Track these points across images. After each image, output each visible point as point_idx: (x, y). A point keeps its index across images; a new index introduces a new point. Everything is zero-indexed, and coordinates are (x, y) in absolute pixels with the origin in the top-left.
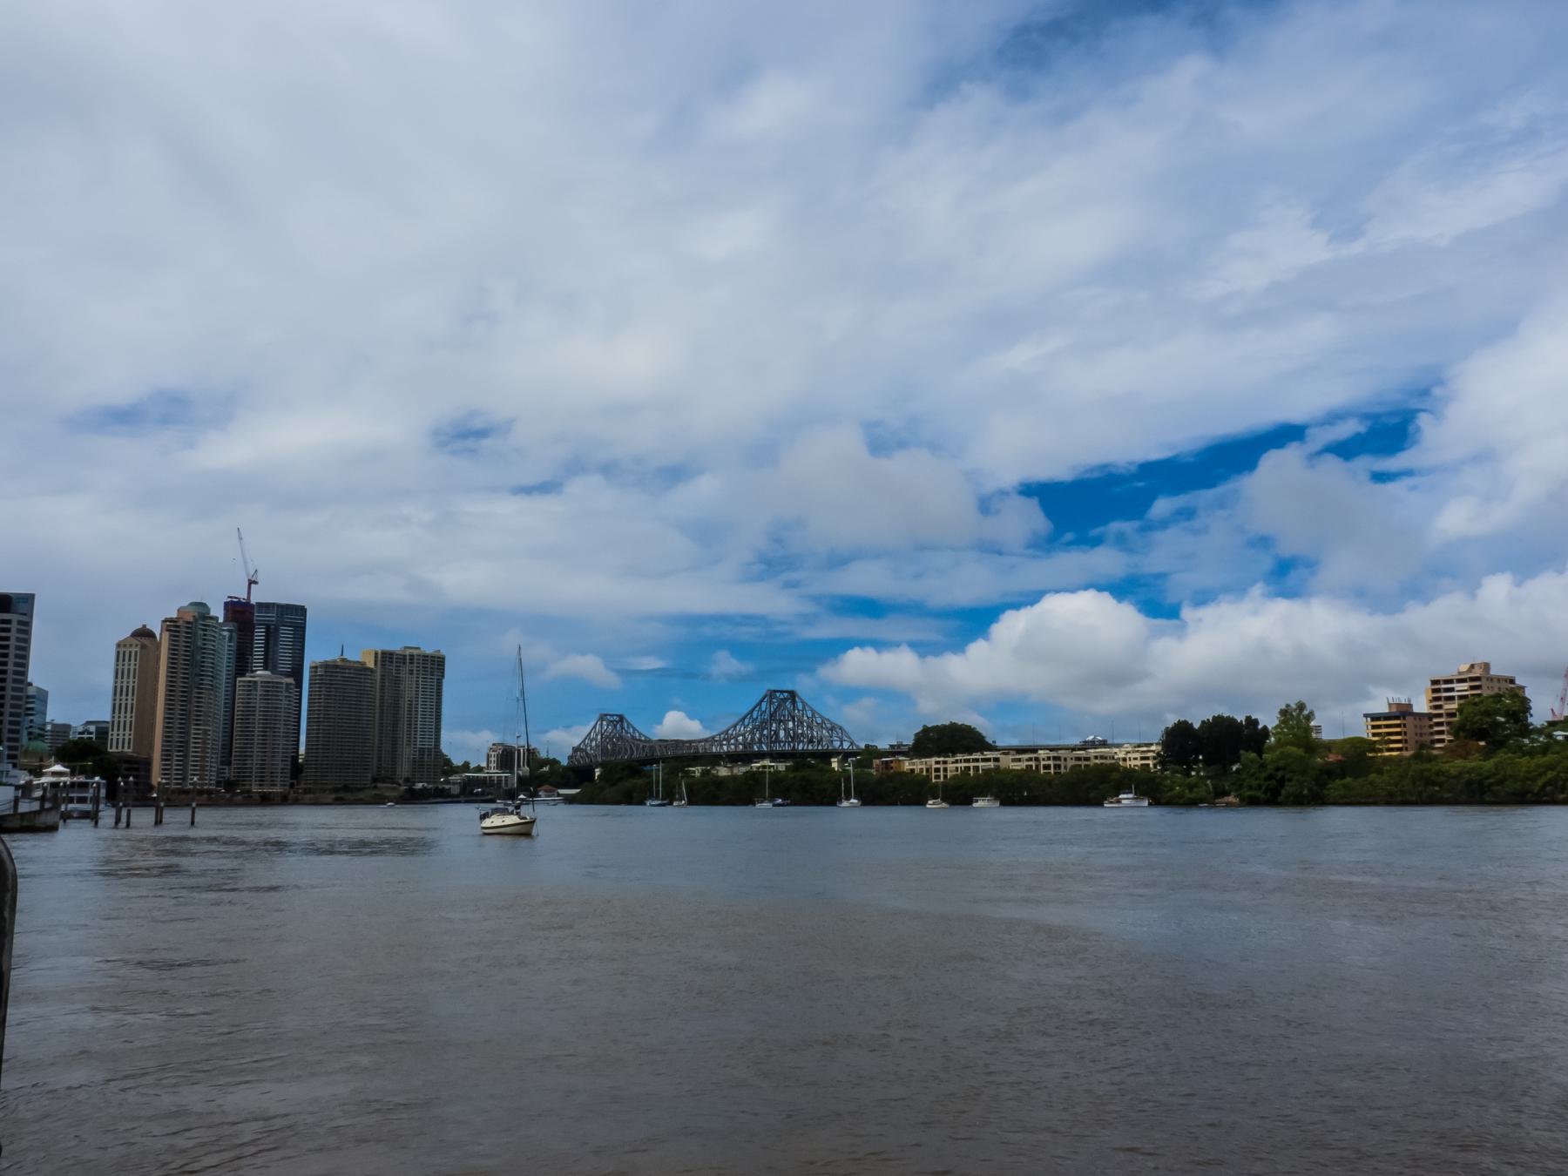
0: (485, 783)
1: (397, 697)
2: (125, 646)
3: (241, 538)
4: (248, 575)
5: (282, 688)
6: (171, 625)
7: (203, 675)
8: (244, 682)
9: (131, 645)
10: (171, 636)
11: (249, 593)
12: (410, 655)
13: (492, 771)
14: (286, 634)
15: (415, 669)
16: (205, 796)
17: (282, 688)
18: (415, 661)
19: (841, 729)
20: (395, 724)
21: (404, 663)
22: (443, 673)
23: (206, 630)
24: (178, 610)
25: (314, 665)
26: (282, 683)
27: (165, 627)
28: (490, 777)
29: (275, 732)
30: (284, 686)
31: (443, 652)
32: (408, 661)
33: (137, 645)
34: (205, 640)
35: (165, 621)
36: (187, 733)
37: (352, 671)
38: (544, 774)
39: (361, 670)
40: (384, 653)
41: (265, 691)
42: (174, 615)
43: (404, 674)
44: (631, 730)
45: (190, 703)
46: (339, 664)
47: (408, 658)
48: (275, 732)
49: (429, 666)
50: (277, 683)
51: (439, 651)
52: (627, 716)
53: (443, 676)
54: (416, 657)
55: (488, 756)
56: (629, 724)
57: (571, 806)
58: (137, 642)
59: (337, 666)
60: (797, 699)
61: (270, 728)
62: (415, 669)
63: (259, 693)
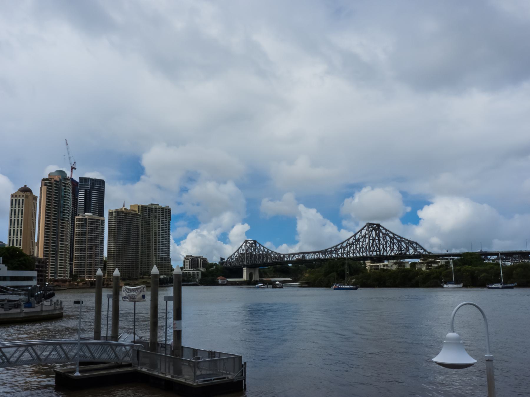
0: (187, 276)
1: (149, 229)
2: (16, 196)
3: (67, 145)
4: (71, 164)
5: (99, 222)
6: (47, 182)
7: (64, 212)
8: (79, 219)
9: (20, 196)
10: (47, 188)
11: (72, 174)
12: (155, 208)
13: (187, 269)
14: (95, 195)
15: (158, 215)
16: (68, 283)
17: (99, 222)
18: (158, 211)
19: (416, 244)
20: (149, 246)
21: (152, 212)
22: (171, 218)
23: (65, 186)
24: (49, 175)
25: (111, 211)
26: (99, 220)
27: (44, 183)
28: (189, 272)
29: (96, 247)
30: (100, 221)
31: (170, 207)
32: (154, 211)
33: (23, 196)
34: (65, 192)
35: (43, 180)
36: (57, 246)
37: (130, 215)
38: (213, 271)
39: (134, 215)
40: (142, 206)
41: (91, 224)
42: (47, 177)
43: (152, 218)
44: (262, 248)
45: (58, 228)
46: (124, 211)
47: (154, 209)
48: (96, 247)
49: (164, 214)
50: (97, 220)
51: (168, 206)
52: (258, 241)
53: (171, 220)
54: (158, 209)
55: (185, 262)
56: (260, 245)
57: (380, 289)
58: (24, 194)
59: (123, 212)
60: (381, 228)
61: (94, 245)
62: (158, 215)
63: (87, 225)
